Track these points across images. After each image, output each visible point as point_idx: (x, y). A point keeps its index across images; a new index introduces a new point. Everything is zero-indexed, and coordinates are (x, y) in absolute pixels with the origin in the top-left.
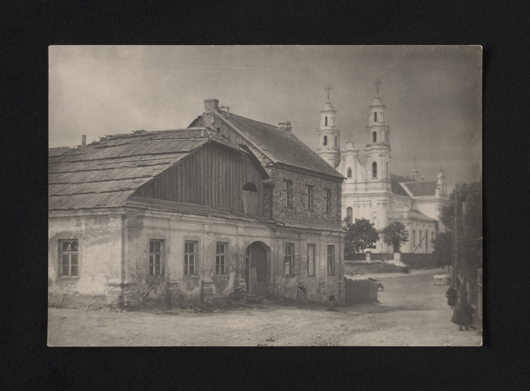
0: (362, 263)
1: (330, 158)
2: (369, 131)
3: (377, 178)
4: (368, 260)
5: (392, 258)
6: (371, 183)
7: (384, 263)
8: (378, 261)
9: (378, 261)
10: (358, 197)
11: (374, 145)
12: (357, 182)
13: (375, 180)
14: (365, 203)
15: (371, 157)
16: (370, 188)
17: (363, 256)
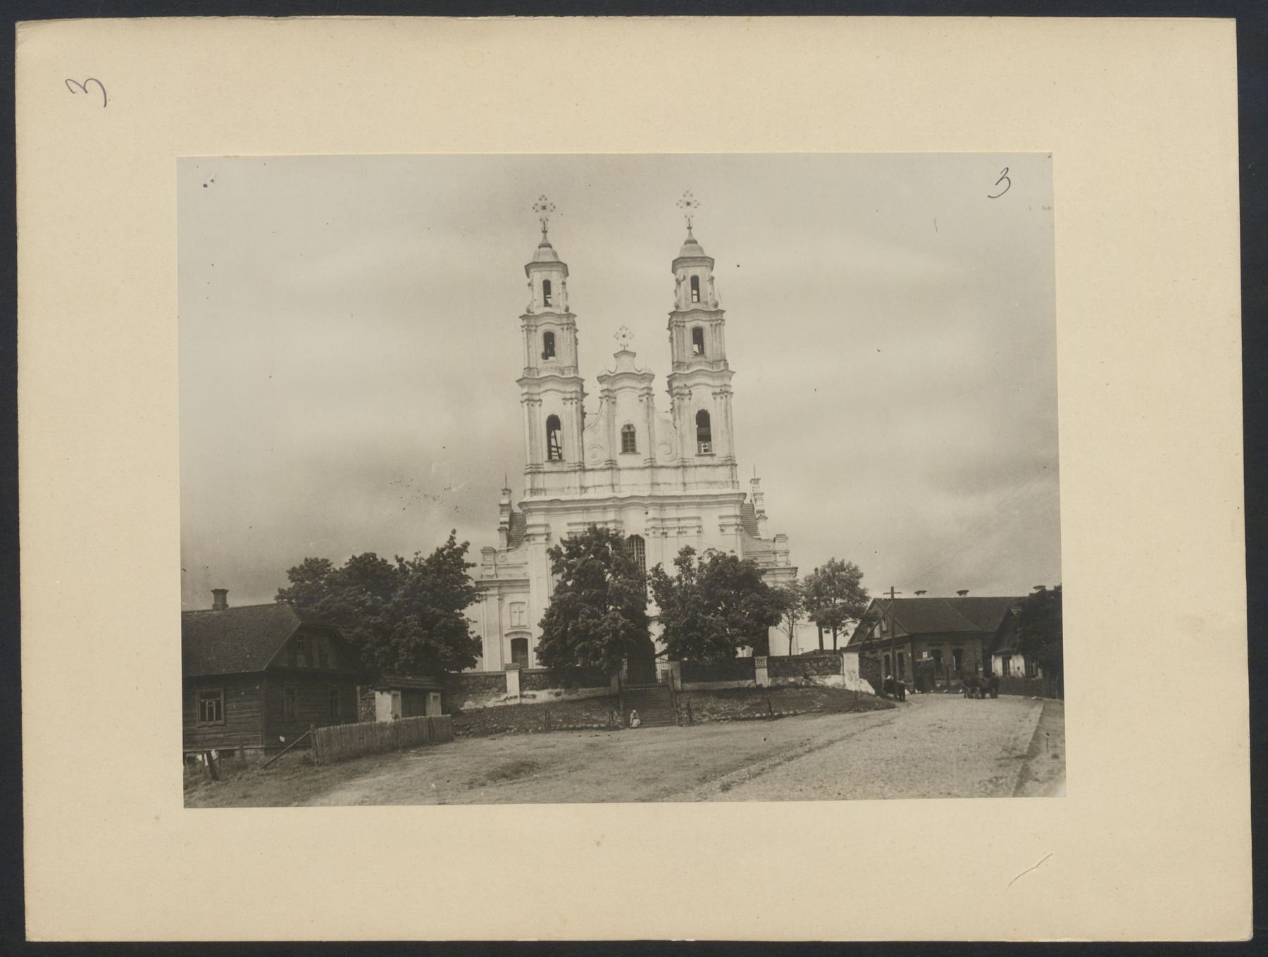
0: (743, 688)
1: (568, 396)
2: (682, 324)
3: (712, 455)
4: (763, 677)
5: (836, 669)
6: (696, 466)
7: (812, 684)
8: (792, 680)
9: (792, 680)
10: (662, 506)
11: (700, 363)
12: (655, 465)
13: (708, 460)
14: (682, 523)
15: (693, 397)
16: (696, 483)
17: (747, 668)
